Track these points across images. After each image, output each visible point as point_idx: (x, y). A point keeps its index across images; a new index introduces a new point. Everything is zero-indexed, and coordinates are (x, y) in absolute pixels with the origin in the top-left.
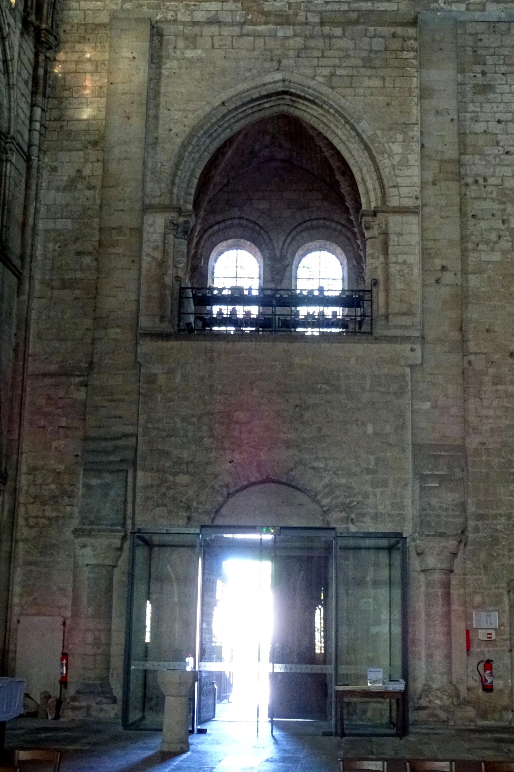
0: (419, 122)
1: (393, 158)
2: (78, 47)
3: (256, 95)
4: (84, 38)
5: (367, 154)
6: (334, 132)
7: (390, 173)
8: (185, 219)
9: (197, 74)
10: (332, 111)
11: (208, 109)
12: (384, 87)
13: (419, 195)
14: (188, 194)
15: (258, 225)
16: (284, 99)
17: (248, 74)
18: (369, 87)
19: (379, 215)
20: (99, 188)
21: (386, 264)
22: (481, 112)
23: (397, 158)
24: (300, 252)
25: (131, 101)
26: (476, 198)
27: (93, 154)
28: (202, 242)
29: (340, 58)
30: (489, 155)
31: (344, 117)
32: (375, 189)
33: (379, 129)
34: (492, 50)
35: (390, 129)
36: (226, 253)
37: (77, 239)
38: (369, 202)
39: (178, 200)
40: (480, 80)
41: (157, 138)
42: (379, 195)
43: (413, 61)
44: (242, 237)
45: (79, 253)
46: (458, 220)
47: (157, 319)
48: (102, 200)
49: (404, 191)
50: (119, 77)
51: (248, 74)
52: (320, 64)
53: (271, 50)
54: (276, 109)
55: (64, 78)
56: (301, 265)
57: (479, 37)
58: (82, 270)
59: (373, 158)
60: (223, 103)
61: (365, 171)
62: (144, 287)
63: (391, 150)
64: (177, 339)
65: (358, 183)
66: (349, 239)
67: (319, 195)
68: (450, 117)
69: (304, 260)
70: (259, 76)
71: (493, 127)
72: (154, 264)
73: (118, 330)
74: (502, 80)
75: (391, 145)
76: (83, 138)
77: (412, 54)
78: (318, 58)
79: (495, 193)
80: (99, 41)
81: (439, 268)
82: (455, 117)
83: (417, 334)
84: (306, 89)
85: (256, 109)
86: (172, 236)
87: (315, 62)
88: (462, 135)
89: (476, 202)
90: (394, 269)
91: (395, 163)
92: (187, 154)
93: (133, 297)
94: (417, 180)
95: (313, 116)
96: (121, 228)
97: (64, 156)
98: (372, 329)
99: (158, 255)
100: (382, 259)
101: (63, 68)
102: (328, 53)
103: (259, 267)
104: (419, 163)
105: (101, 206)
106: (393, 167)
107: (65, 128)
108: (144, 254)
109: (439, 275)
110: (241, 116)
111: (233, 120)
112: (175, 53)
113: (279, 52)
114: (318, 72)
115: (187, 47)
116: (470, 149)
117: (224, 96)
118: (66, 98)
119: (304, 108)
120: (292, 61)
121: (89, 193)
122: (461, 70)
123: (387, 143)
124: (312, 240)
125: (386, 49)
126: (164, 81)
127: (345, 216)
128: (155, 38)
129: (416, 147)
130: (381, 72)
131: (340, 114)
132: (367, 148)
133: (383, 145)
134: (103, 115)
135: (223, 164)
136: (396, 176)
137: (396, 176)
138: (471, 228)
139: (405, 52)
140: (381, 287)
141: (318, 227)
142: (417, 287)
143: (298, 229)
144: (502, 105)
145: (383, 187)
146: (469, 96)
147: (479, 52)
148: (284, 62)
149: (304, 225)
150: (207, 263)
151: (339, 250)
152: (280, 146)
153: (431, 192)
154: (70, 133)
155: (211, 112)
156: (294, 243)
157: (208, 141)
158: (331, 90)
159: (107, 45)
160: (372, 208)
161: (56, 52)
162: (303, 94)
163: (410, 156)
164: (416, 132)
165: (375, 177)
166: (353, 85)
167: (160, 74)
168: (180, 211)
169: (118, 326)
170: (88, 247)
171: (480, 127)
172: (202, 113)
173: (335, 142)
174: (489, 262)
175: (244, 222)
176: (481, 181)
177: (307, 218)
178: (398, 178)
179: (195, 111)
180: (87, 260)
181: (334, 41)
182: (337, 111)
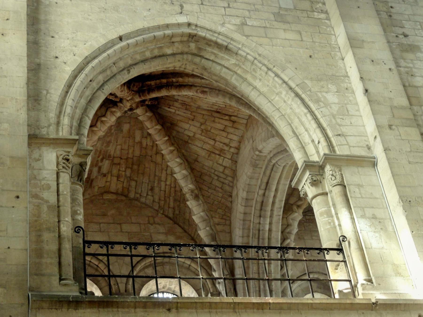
1: (331, 107)
23: (335, 108)
25: (6, 18)
35: (320, 80)
49: (352, 140)
57: (390, 5)
68: (387, 67)
75: (324, 94)
78: (225, 8)
82: (393, 67)
91: (335, 113)
119: (212, 58)
123: (320, 92)
125: (295, 9)
133: (316, 94)
137: (340, 125)
147: (395, 17)
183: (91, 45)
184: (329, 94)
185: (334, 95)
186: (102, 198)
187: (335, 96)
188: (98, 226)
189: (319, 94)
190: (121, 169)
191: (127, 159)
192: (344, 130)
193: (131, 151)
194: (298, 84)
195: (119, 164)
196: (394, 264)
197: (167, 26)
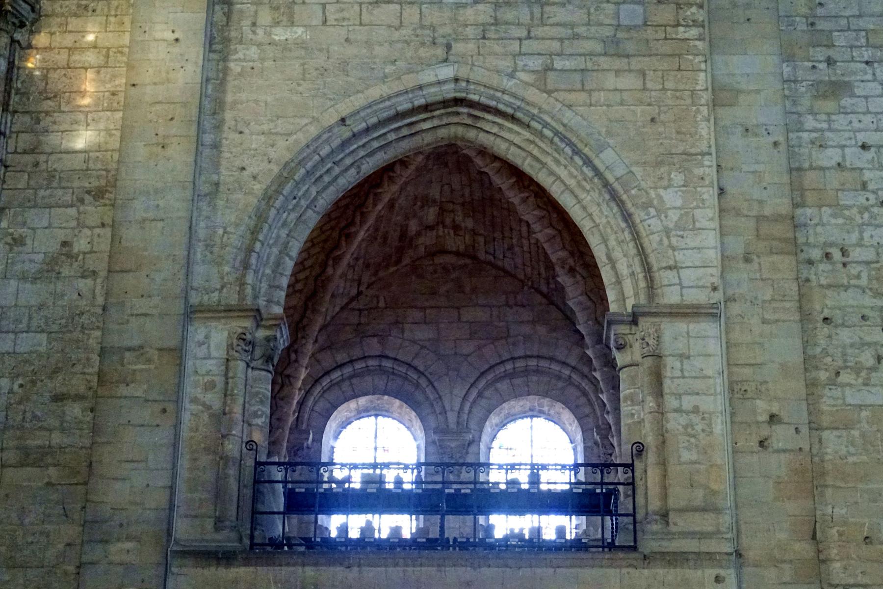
0: (713, 150)
1: (666, 217)
2: (74, 23)
3: (405, 106)
4: (86, 7)
5: (616, 209)
6: (552, 173)
7: (661, 242)
8: (268, 333)
9: (296, 69)
10: (548, 133)
11: (313, 131)
12: (645, 89)
13: (716, 280)
14: (273, 287)
15: (415, 369)
16: (458, 114)
17: (389, 69)
18: (616, 90)
19: (643, 322)
20: (103, 274)
21: (660, 412)
22: (830, 129)
23: (674, 216)
24: (494, 419)
25: (170, 117)
26: (829, 286)
27: (93, 212)
28: (310, 403)
29: (561, 40)
30: (848, 207)
31: (570, 144)
32: (633, 274)
33: (637, 163)
34: (843, 22)
35: (659, 164)
36: (356, 424)
37: (56, 371)
38: (623, 298)
39: (256, 297)
40: (824, 72)
41: (217, 184)
42: (642, 284)
43: (697, 43)
44: (385, 393)
45: (58, 398)
46: (796, 327)
47: (209, 524)
48: (107, 294)
49: (688, 276)
50: (146, 75)
51: (389, 69)
52: (523, 50)
53: (433, 28)
54: (443, 133)
55: (45, 78)
56: (495, 444)
58: (63, 430)
59: (627, 217)
60: (343, 120)
61: (612, 243)
62: (184, 463)
64: (247, 562)
65: (600, 265)
66: (585, 394)
67: (526, 315)
68: (771, 139)
69: (502, 434)
70: (410, 71)
71: (853, 157)
72: (205, 417)
73: (129, 545)
74: (866, 73)
75: (661, 192)
76: (76, 184)
77: (694, 32)
78: (520, 39)
79: (864, 275)
80: (113, 13)
81: (765, 417)
82: (781, 139)
83: (727, 548)
84: (499, 94)
85: (405, 132)
86: (241, 365)
87: (515, 46)
88: (795, 171)
89: (829, 293)
90: (674, 423)
91: (671, 226)
92: (273, 212)
93: (163, 481)
94: (713, 255)
95: (512, 143)
96: (141, 347)
97: (37, 218)
98: (635, 541)
99: (213, 399)
100: (651, 403)
101: (43, 60)
102: (538, 31)
103: (418, 447)
104: (715, 224)
105: (104, 308)
106: (667, 232)
107: (43, 166)
108: (186, 401)
109: (765, 431)
110: (376, 144)
111: (362, 153)
112: (254, 32)
113: (448, 30)
114: (520, 64)
115: (277, 23)
116: (810, 197)
117: (345, 108)
118: (47, 113)
119: (495, 130)
120: (471, 46)
121: (84, 285)
122: (789, 58)
123: (656, 188)
124: (517, 396)
125: (645, 24)
126: (231, 83)
127: (577, 351)
128: (217, 8)
129: (709, 194)
130: (636, 63)
131: (563, 139)
132: (614, 197)
133: (647, 193)
134: (115, 143)
135: (347, 259)
137: (674, 249)
138: (823, 342)
139: (681, 29)
140: (651, 457)
141: (526, 372)
142: (722, 457)
143: (490, 376)
144: (867, 119)
145: (648, 269)
146: (806, 102)
147: (821, 25)
148: (458, 47)
149: (501, 370)
150: (318, 440)
151: (567, 416)
152: (456, 228)
153: (741, 275)
154: (51, 175)
155: (319, 137)
156: (483, 402)
157: (314, 191)
159: (127, 20)
160: (629, 310)
161: (32, 32)
162: (493, 103)
163: (698, 213)
164: (707, 168)
165: (633, 251)
166: (587, 88)
167: (226, 71)
168: (257, 315)
169: (129, 538)
170: (79, 385)
171: (831, 157)
172: (302, 138)
173: (555, 190)
174: (860, 407)
175: (387, 364)
176: (837, 254)
177: (506, 356)
178: (676, 253)
179: (290, 135)
180: (75, 410)
181: (547, 9)
182: (556, 133)
183: (296, 141)
184: (669, 190)
185: (676, 192)
186: (431, 262)
187: (680, 193)
188: (422, 314)
189: (653, 194)
191: (463, 204)
193: (467, 192)
194: (619, 176)
195: (452, 211)
196: (709, 488)
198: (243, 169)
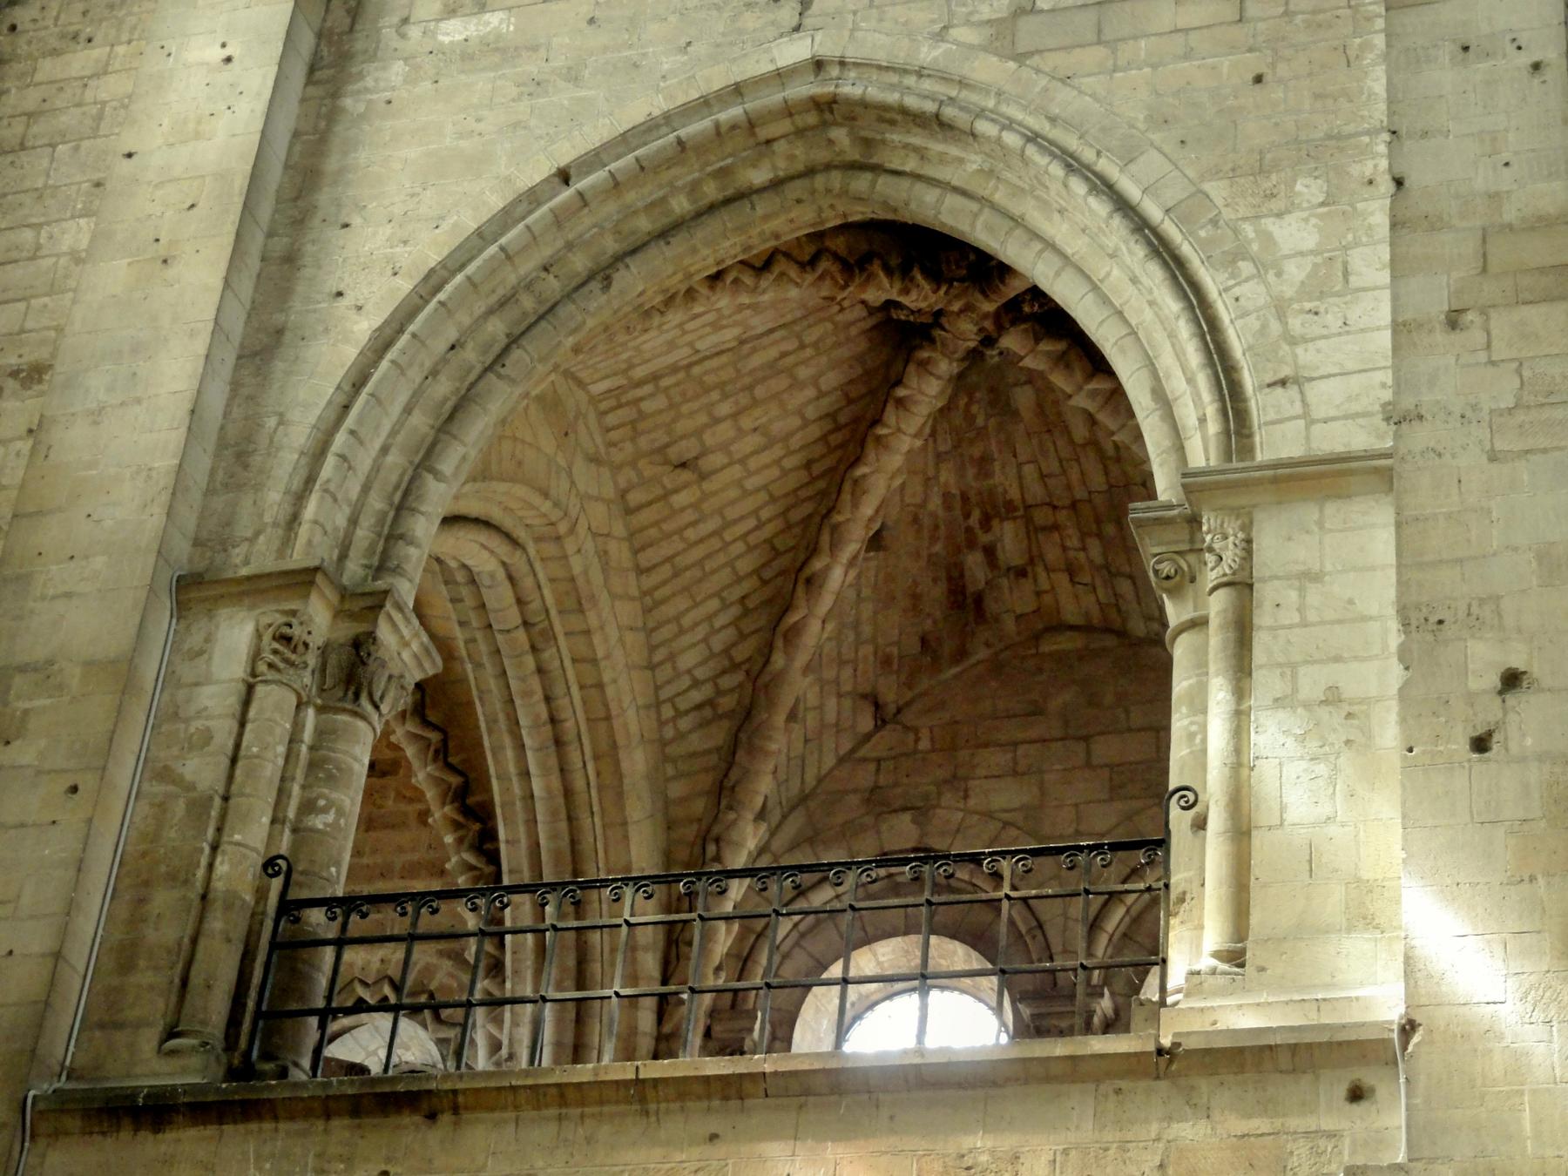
1: (1279, 274)
18: (1177, 31)
23: (1296, 272)
33: (1215, 173)
63: (1267, 239)
68: (1525, 59)
75: (1269, 224)
80: (125, 37)
91: (1289, 292)
109: (1489, 712)
112: (403, 36)
119: (911, 165)
133: (1236, 231)
136: (1293, 341)
137: (1293, 341)
158: (1012, 65)
166: (1108, 35)
178: (1299, 350)
182: (1033, 138)
183: (455, 225)
184: (1288, 218)
185: (1306, 220)
186: (1033, 651)
187: (1313, 221)
188: (1009, 756)
189: (1248, 229)
190: (1068, 544)
191: (1074, 505)
192: (1306, 356)
193: (1074, 474)
194: (1170, 204)
195: (1056, 527)
196: (1359, 880)
197: (737, 91)
198: (340, 294)
